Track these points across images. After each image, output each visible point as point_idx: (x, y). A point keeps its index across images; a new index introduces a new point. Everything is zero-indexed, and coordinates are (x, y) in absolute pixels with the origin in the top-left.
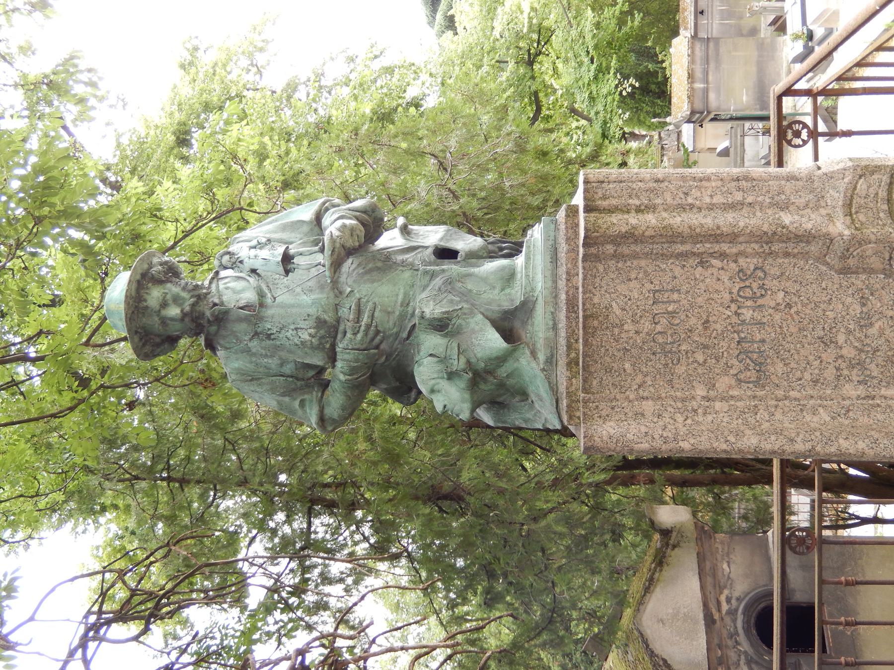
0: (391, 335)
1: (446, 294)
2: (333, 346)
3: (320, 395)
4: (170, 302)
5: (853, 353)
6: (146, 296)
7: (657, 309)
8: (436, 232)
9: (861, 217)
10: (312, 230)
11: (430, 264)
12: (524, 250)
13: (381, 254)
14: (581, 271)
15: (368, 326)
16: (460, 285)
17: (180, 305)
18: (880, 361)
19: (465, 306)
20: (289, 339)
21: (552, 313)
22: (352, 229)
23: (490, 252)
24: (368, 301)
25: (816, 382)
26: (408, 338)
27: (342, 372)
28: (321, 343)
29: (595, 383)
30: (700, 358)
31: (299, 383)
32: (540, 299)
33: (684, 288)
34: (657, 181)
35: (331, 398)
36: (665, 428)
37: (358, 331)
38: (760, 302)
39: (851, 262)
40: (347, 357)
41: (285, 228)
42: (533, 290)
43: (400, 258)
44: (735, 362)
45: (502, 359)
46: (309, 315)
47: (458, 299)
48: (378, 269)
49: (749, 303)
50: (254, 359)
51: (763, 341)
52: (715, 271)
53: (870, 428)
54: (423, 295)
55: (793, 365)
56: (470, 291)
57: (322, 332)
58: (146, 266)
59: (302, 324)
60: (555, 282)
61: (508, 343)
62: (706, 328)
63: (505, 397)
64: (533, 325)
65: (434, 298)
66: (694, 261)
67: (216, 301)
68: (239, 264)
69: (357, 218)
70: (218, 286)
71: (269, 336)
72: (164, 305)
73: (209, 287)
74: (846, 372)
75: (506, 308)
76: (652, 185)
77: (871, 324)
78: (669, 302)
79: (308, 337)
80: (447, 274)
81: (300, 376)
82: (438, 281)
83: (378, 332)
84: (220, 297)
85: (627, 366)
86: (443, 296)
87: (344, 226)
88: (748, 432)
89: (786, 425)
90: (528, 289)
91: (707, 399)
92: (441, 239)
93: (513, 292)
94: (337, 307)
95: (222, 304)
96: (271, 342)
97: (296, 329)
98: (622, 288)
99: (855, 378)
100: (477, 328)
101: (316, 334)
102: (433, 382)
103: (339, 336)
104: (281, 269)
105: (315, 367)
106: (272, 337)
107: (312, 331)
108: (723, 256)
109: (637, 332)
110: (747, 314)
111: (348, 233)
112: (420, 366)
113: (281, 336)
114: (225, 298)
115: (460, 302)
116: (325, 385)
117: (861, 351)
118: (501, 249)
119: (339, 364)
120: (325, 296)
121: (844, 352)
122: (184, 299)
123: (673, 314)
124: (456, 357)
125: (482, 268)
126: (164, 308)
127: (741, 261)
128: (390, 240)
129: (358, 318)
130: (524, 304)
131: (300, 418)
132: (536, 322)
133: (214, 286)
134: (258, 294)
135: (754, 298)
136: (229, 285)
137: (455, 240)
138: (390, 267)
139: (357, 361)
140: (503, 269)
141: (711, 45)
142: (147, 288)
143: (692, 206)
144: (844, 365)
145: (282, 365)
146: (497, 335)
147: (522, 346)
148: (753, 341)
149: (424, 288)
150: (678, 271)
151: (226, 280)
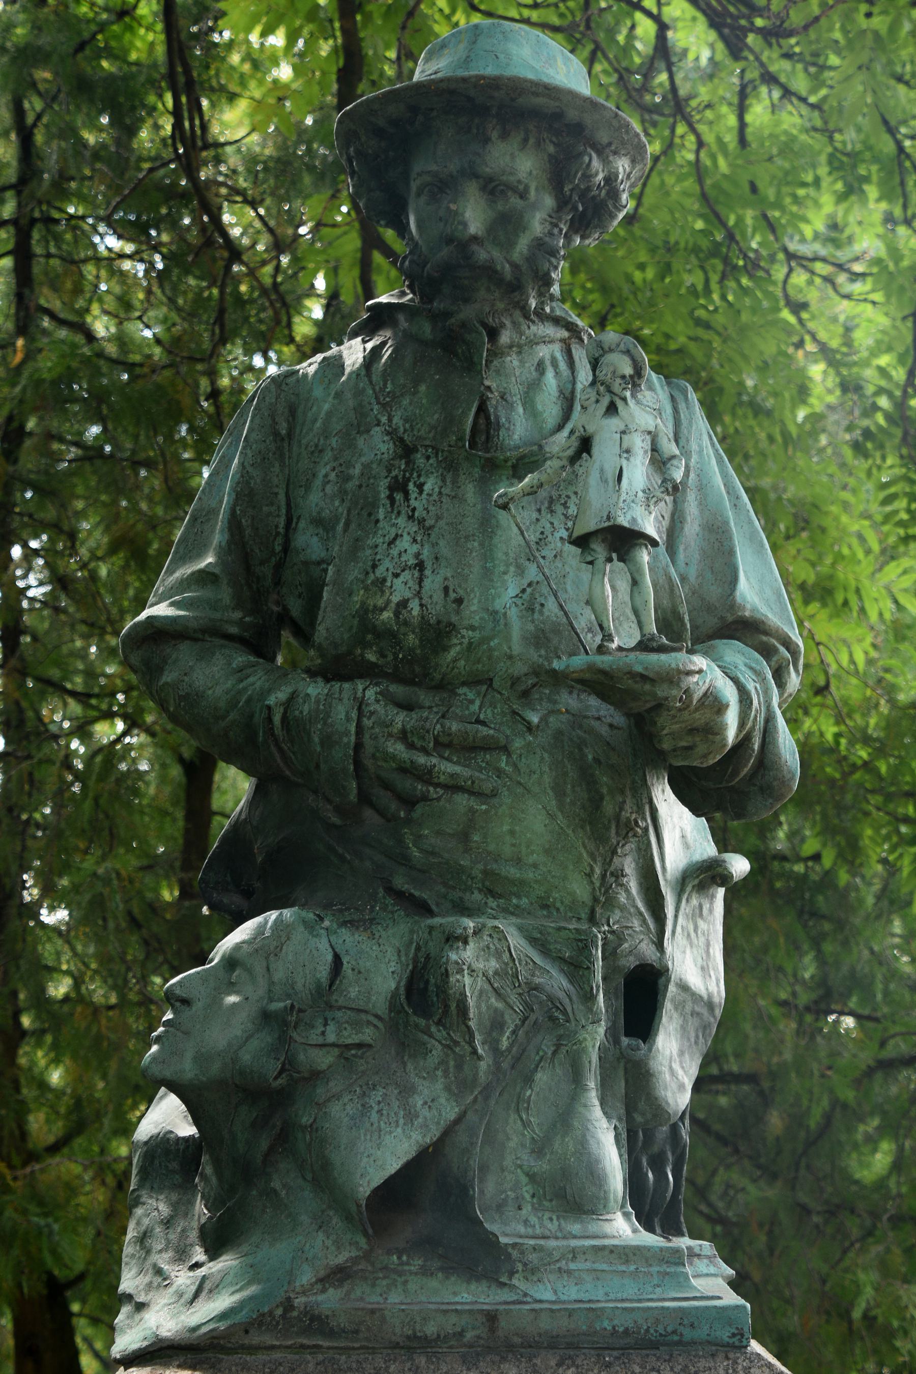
1: (518, 1007)
2: (369, 672)
3: (233, 630)
8: (704, 970)
10: (710, 609)
13: (640, 810)
15: (426, 776)
16: (548, 1048)
19: (483, 1065)
20: (392, 543)
21: (461, 1334)
23: (649, 1136)
24: (500, 773)
26: (391, 890)
27: (293, 697)
31: (267, 571)
32: (505, 1295)
37: (411, 746)
42: (531, 1271)
43: (629, 866)
46: (459, 601)
47: (505, 1043)
54: (515, 940)
56: (528, 1080)
57: (412, 640)
58: (603, 137)
59: (433, 583)
64: (425, 1272)
65: (508, 972)
67: (505, 338)
68: (605, 401)
69: (743, 743)
70: (546, 341)
71: (399, 486)
80: (579, 1007)
83: (410, 802)
86: (513, 998)
87: (720, 708)
90: (533, 1257)
92: (684, 987)
93: (527, 1210)
95: (495, 354)
96: (384, 494)
97: (420, 566)
100: (418, 1101)
101: (406, 623)
103: (395, 689)
104: (590, 523)
105: (312, 624)
106: (399, 497)
111: (700, 718)
113: (401, 521)
115: (495, 1050)
118: (657, 1164)
119: (315, 689)
120: (517, 647)
122: (510, 244)
124: (331, 1038)
125: (597, 1112)
126: (483, 189)
129: (449, 745)
130: (490, 1243)
132: (434, 1283)
133: (549, 330)
134: (521, 458)
136: (550, 375)
137: (683, 1028)
138: (600, 838)
139: (328, 741)
145: (318, 522)
146: (393, 1166)
147: (363, 1242)
149: (539, 942)
151: (563, 366)
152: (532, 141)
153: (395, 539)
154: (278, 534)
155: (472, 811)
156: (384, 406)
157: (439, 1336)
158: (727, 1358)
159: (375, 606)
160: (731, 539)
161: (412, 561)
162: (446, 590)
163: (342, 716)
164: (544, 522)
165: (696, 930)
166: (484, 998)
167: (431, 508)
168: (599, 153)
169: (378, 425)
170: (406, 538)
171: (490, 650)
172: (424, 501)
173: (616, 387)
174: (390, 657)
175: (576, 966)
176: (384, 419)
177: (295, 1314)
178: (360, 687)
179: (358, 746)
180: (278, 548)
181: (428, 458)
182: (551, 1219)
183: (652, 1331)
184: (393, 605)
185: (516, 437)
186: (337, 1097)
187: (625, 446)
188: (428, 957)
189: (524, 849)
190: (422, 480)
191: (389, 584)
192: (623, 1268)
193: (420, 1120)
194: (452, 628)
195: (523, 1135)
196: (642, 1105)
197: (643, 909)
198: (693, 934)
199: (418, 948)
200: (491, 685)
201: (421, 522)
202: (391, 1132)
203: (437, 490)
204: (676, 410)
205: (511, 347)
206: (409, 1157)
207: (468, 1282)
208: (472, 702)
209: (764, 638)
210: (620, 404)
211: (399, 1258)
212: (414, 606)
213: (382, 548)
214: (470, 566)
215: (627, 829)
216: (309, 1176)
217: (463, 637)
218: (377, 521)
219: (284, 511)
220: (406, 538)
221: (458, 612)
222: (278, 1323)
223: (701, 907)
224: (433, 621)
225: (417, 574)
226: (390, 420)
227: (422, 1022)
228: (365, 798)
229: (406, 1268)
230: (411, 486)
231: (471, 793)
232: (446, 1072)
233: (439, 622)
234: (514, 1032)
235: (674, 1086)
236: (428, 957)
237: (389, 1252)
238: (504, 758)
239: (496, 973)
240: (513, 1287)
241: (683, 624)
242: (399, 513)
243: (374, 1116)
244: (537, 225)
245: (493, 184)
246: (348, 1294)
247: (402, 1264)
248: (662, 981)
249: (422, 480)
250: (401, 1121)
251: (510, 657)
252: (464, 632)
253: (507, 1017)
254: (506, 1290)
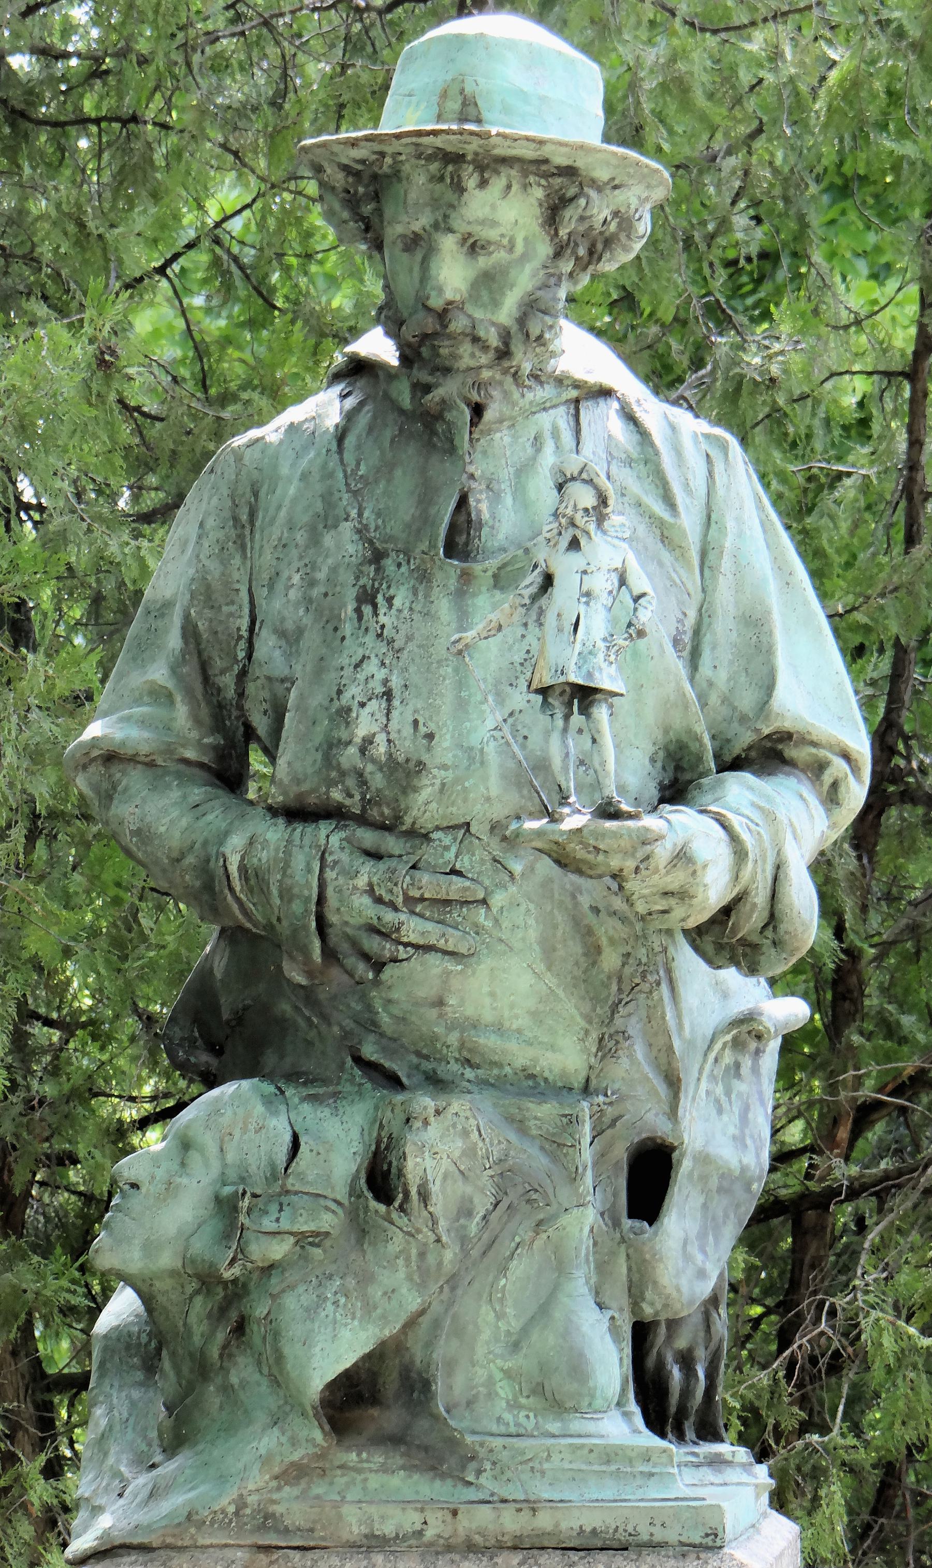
0: (369, 1007)
4: (483, 262)
6: (497, 184)
12: (655, 1441)
21: (420, 1533)
24: (478, 930)
26: (359, 1060)
28: (343, 774)
31: (228, 682)
35: (175, 794)
37: (379, 900)
40: (299, 861)
46: (430, 736)
48: (593, 951)
50: (301, 537)
56: (503, 1270)
57: (377, 781)
58: (602, 175)
59: (401, 718)
61: (332, 1386)
63: (171, 1374)
64: (384, 1469)
67: (489, 415)
71: (367, 597)
75: (439, 1387)
79: (361, 731)
81: (251, 688)
92: (704, 1159)
96: (351, 607)
97: (388, 695)
100: (376, 1293)
101: (373, 761)
102: (212, 1148)
106: (367, 610)
107: (380, 749)
111: (674, 881)
112: (268, 1101)
113: (370, 639)
122: (496, 304)
131: (121, 676)
136: (549, 447)
139: (287, 894)
142: (526, 187)
151: (567, 437)
152: (515, 187)
153: (362, 661)
154: (240, 637)
155: (448, 973)
156: (355, 493)
157: (397, 1535)
158: (698, 1558)
159: (340, 741)
160: (771, 634)
161: (380, 689)
162: (416, 723)
163: (302, 866)
164: (531, 639)
165: (728, 1093)
166: (449, 1182)
167: (401, 626)
168: (599, 190)
169: (346, 520)
170: (375, 661)
171: (465, 789)
172: (394, 619)
173: (580, 519)
174: (358, 797)
175: (559, 1145)
176: (354, 513)
177: (248, 1511)
178: (323, 833)
179: (321, 900)
180: (241, 655)
181: (399, 565)
182: (528, 1417)
183: (621, 1530)
184: (358, 740)
185: (501, 536)
186: (292, 1287)
187: (585, 589)
188: (390, 1137)
189: (506, 1014)
190: (392, 592)
191: (354, 715)
192: (604, 1468)
193: (379, 1311)
195: (498, 1328)
196: (649, 1294)
197: (651, 1076)
198: (723, 1098)
199: (381, 1127)
200: (468, 830)
201: (390, 642)
202: (346, 1325)
203: (407, 605)
204: (711, 474)
205: (501, 421)
206: (367, 1350)
207: (433, 1479)
208: (447, 848)
209: (814, 750)
210: (583, 542)
211: (358, 1455)
212: (381, 739)
213: (348, 671)
214: (442, 695)
216: (265, 1370)
217: (434, 777)
218: (343, 638)
219: (246, 611)
220: (375, 661)
221: (429, 749)
222: (231, 1521)
223: (737, 1065)
224: (401, 759)
225: (384, 705)
226: (360, 515)
227: (382, 1208)
229: (366, 1465)
230: (380, 599)
231: (446, 953)
232: (408, 1260)
233: (408, 760)
234: (484, 1217)
235: (690, 1271)
236: (390, 1137)
237: (349, 1449)
238: (483, 911)
239: (464, 1153)
240: (479, 1487)
241: (702, 744)
242: (367, 630)
243: (330, 1307)
245: (471, 241)
246: (304, 1492)
247: (361, 1461)
248: (675, 1155)
249: (392, 592)
250: (358, 1315)
251: (488, 799)
252: (435, 771)
253: (476, 1201)
254: (472, 1489)
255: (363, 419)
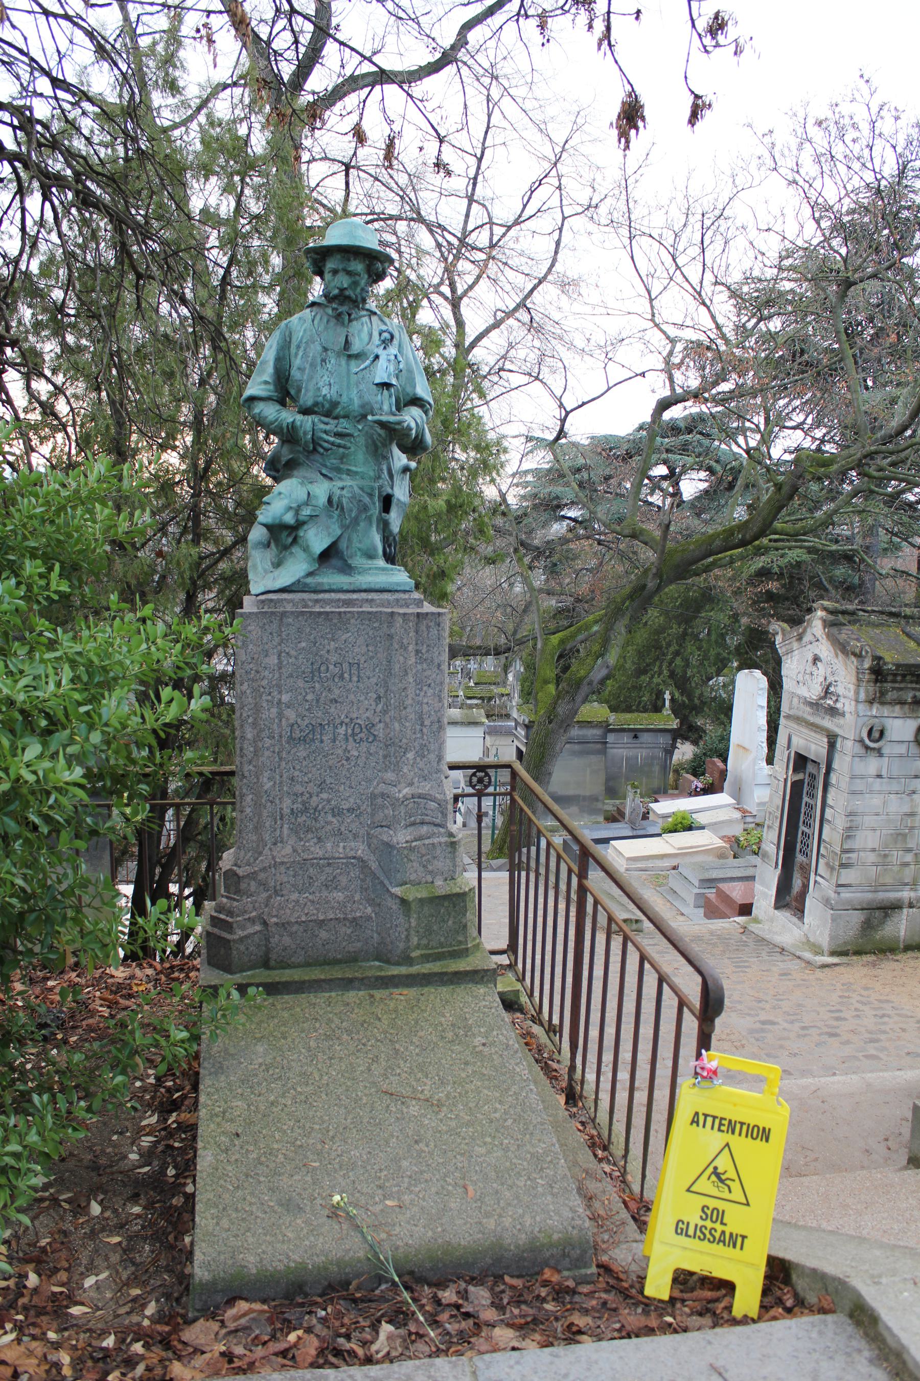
5: (314, 805)
7: (346, 666)
9: (411, 805)
11: (380, 493)
12: (390, 566)
14: (374, 610)
17: (350, 286)
18: (308, 823)
22: (409, 435)
25: (292, 779)
29: (290, 620)
30: (309, 697)
33: (360, 684)
34: (439, 665)
36: (257, 672)
38: (351, 739)
39: (379, 800)
41: (410, 371)
44: (307, 722)
45: (306, 549)
49: (350, 731)
51: (322, 741)
52: (373, 707)
53: (260, 816)
54: (356, 488)
55: (305, 763)
60: (365, 591)
62: (331, 701)
65: (354, 497)
66: (382, 692)
69: (417, 437)
71: (323, 360)
72: (349, 273)
73: (363, 309)
74: (300, 800)
76: (436, 661)
77: (334, 816)
78: (350, 675)
82: (366, 499)
83: (327, 450)
84: (356, 319)
85: (303, 644)
88: (255, 732)
89: (261, 759)
91: (280, 702)
94: (346, 417)
95: (350, 321)
98: (361, 640)
99: (295, 806)
105: (298, 397)
108: (385, 712)
109: (328, 651)
110: (342, 730)
114: (355, 323)
116: (283, 403)
117: (315, 810)
118: (390, 546)
119: (299, 417)
121: (315, 798)
123: (342, 677)
127: (381, 725)
128: (400, 459)
133: (365, 313)
135: (353, 735)
139: (305, 433)
140: (375, 549)
141: (599, 746)
143: (421, 690)
144: (305, 798)
148: (321, 734)
149: (362, 489)
150: (373, 680)
194: (339, 403)
215: (385, 458)
228: (315, 449)
244: (363, 283)
255: (318, 317)
